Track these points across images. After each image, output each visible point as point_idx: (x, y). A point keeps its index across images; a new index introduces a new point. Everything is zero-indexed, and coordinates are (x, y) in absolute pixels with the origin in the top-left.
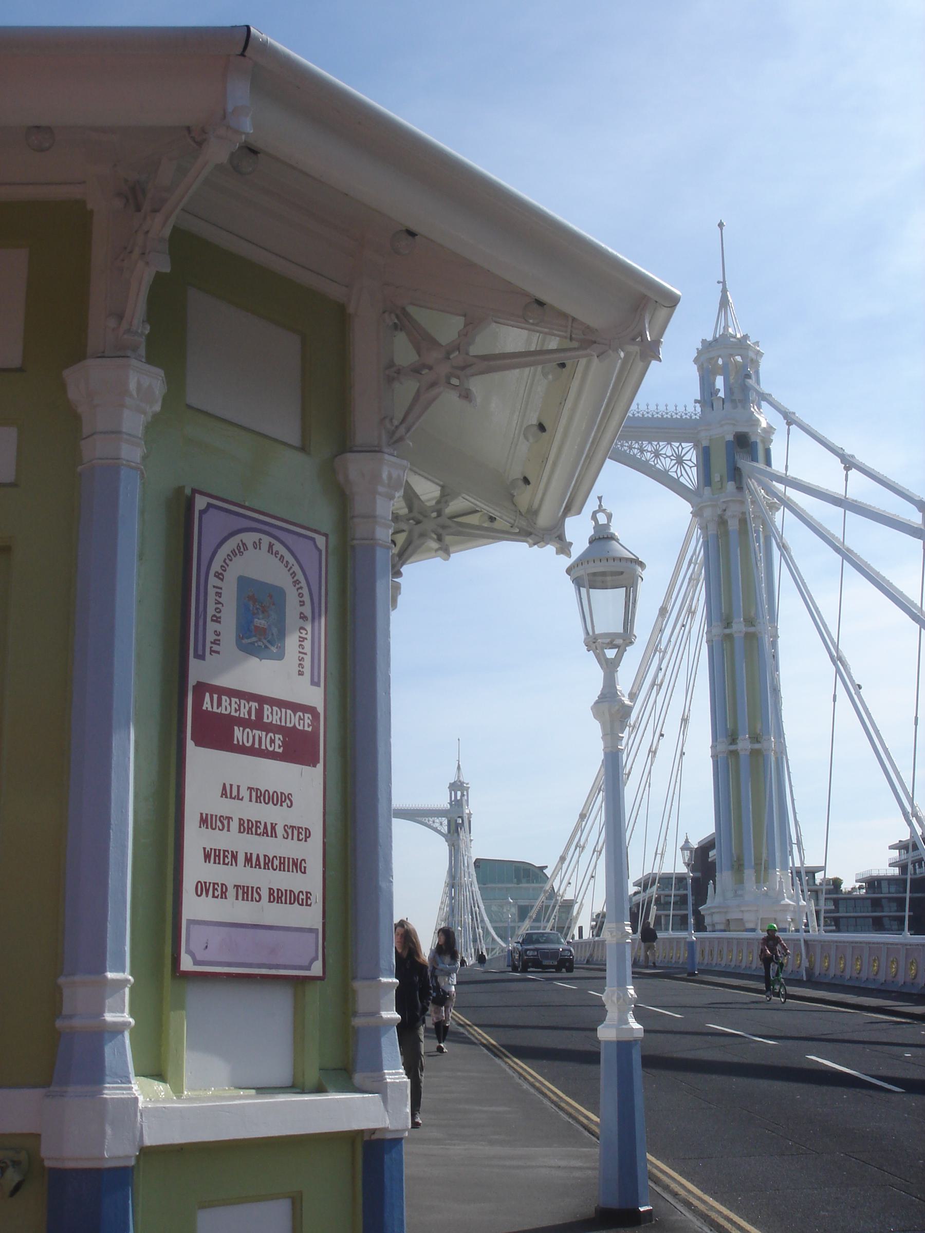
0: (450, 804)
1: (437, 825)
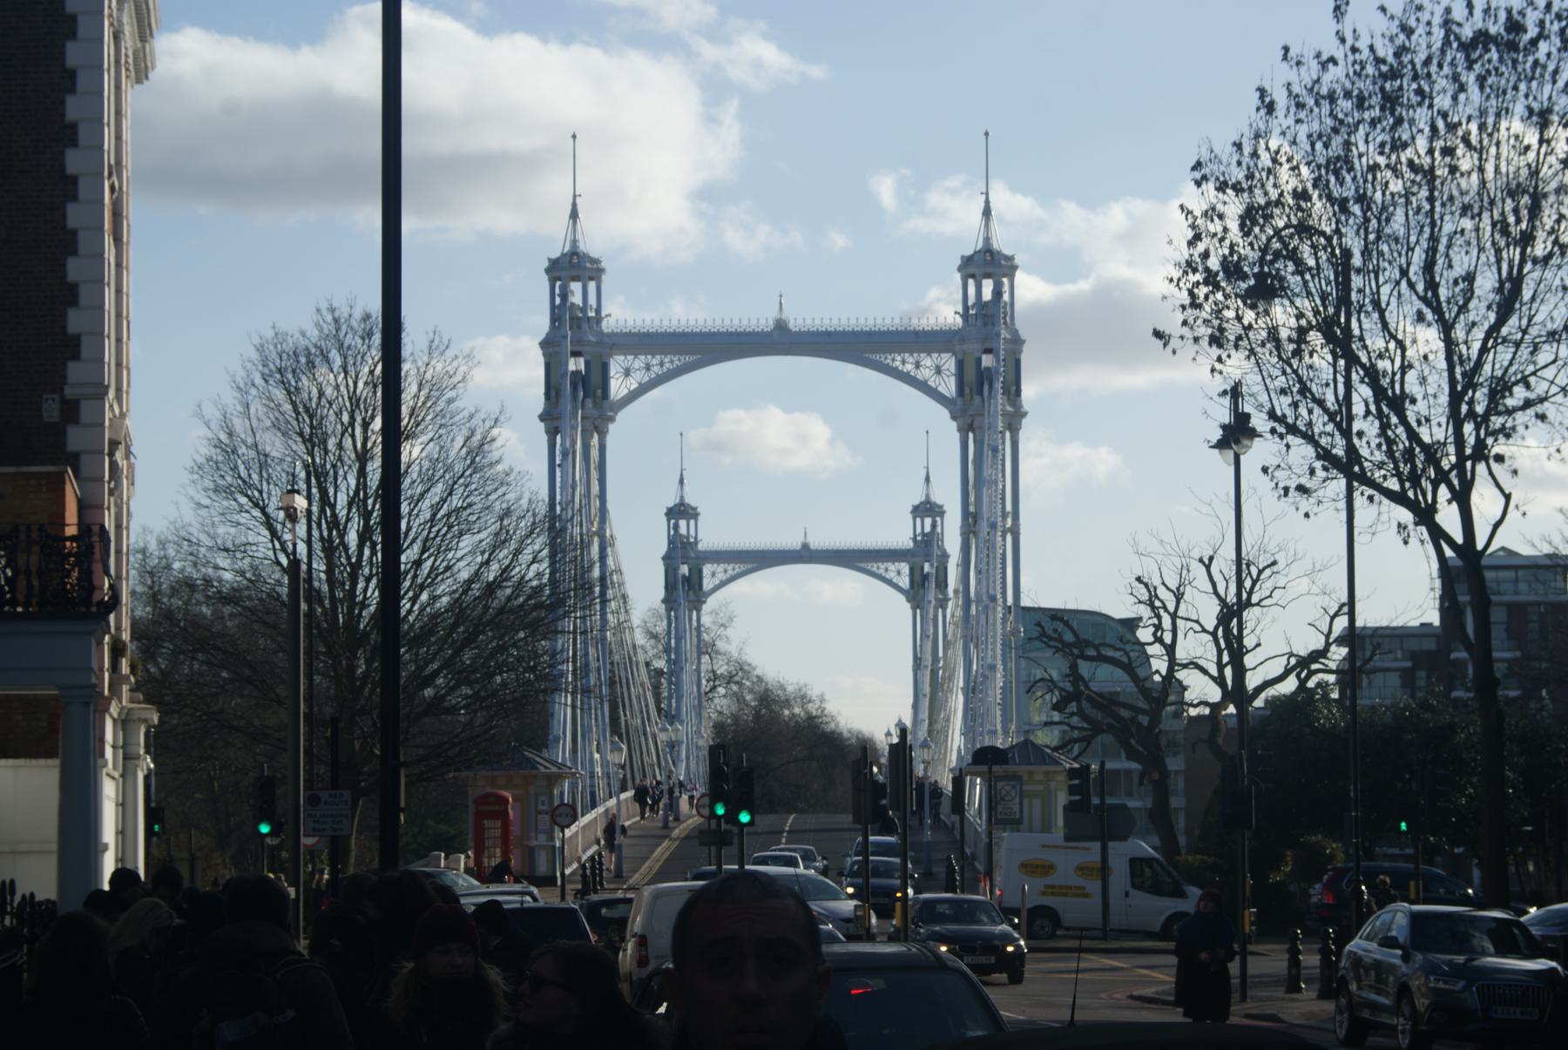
0: (914, 539)
1: (891, 575)
